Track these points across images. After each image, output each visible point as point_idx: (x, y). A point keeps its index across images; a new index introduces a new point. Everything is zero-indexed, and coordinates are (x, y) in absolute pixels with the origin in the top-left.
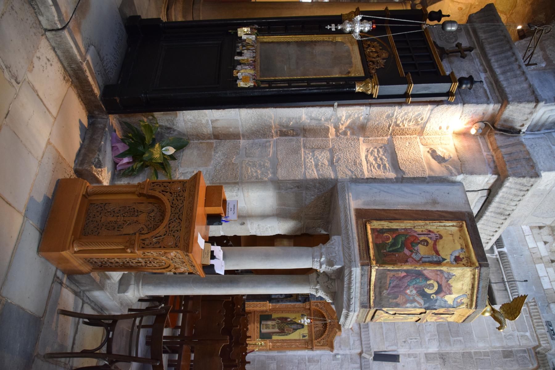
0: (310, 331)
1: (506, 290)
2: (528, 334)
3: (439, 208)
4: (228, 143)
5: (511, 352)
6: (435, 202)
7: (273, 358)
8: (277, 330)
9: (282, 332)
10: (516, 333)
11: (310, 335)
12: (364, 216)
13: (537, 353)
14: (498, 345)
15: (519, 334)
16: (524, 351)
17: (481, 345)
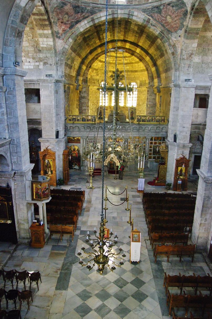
0: (50, 159)
1: (34, 83)
2: (50, 85)
3: (31, 186)
4: (19, 221)
5: (56, 90)
6: (30, 187)
7: (58, 169)
8: (50, 169)
9: (50, 167)
10: (50, 89)
11: (51, 159)
12: (33, 199)
13: (56, 82)
14: (54, 97)
15: (50, 88)
16: (56, 85)
17: (53, 103)
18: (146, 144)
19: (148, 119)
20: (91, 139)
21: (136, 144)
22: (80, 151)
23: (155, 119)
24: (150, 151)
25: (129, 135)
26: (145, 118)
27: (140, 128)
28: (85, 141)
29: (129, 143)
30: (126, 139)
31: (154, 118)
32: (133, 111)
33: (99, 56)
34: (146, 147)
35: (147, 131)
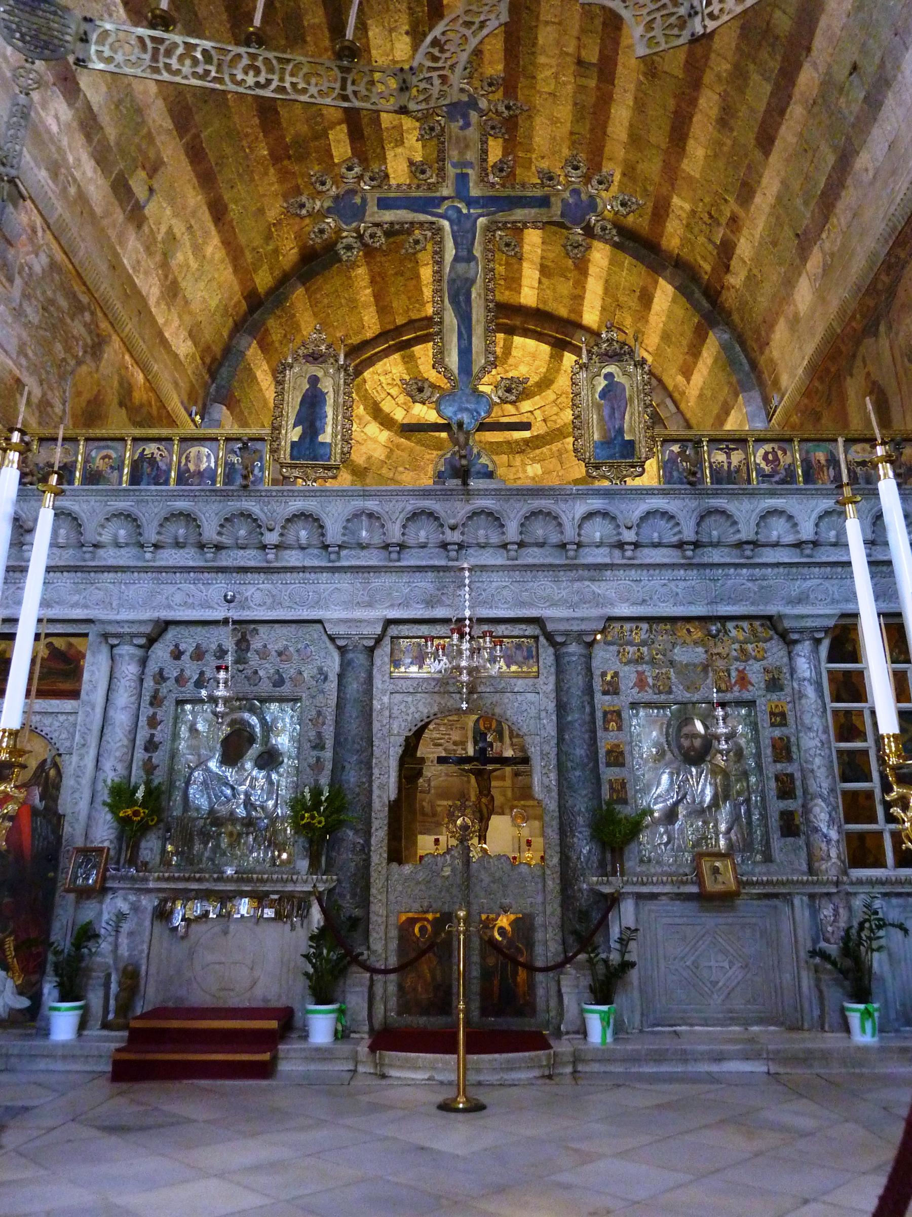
18: (802, 696)
19: (767, 469)
20: (199, 654)
21: (680, 693)
22: (68, 782)
23: (833, 461)
24: (845, 779)
25: (597, 600)
26: (737, 457)
27: (715, 530)
28: (129, 670)
29: (612, 689)
30: (573, 648)
31: (821, 456)
32: (620, 378)
33: (371, 362)
34: (802, 727)
35: (784, 556)
